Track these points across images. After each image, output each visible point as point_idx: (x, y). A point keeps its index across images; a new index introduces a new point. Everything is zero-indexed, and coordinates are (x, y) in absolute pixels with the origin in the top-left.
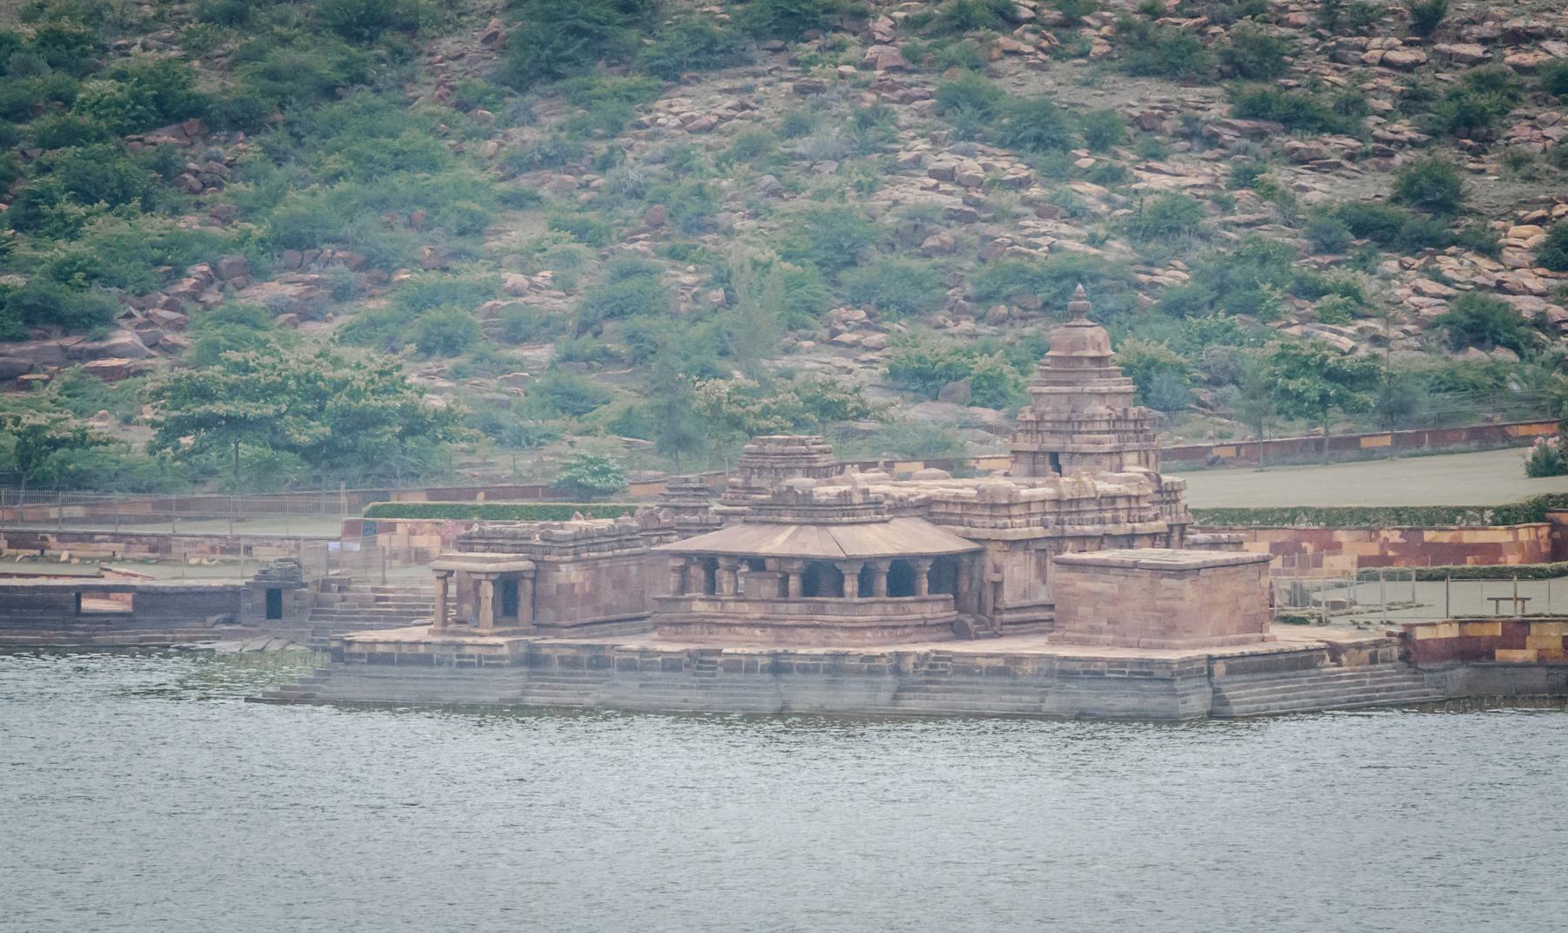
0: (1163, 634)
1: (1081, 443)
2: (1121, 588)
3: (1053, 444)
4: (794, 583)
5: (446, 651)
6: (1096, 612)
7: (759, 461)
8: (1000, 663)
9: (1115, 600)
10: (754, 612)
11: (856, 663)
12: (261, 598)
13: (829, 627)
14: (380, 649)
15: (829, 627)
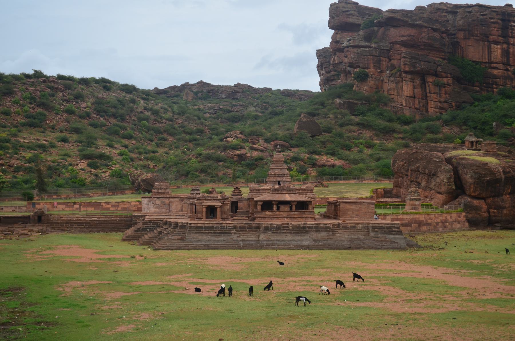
0: (371, 218)
1: (284, 179)
2: (360, 208)
3: (279, 179)
4: (294, 207)
5: (217, 225)
6: (353, 213)
7: (159, 187)
8: (354, 225)
9: (358, 211)
10: (285, 215)
11: (322, 225)
12: (36, 218)
13: (307, 217)
14: (199, 225)
15: (307, 217)
